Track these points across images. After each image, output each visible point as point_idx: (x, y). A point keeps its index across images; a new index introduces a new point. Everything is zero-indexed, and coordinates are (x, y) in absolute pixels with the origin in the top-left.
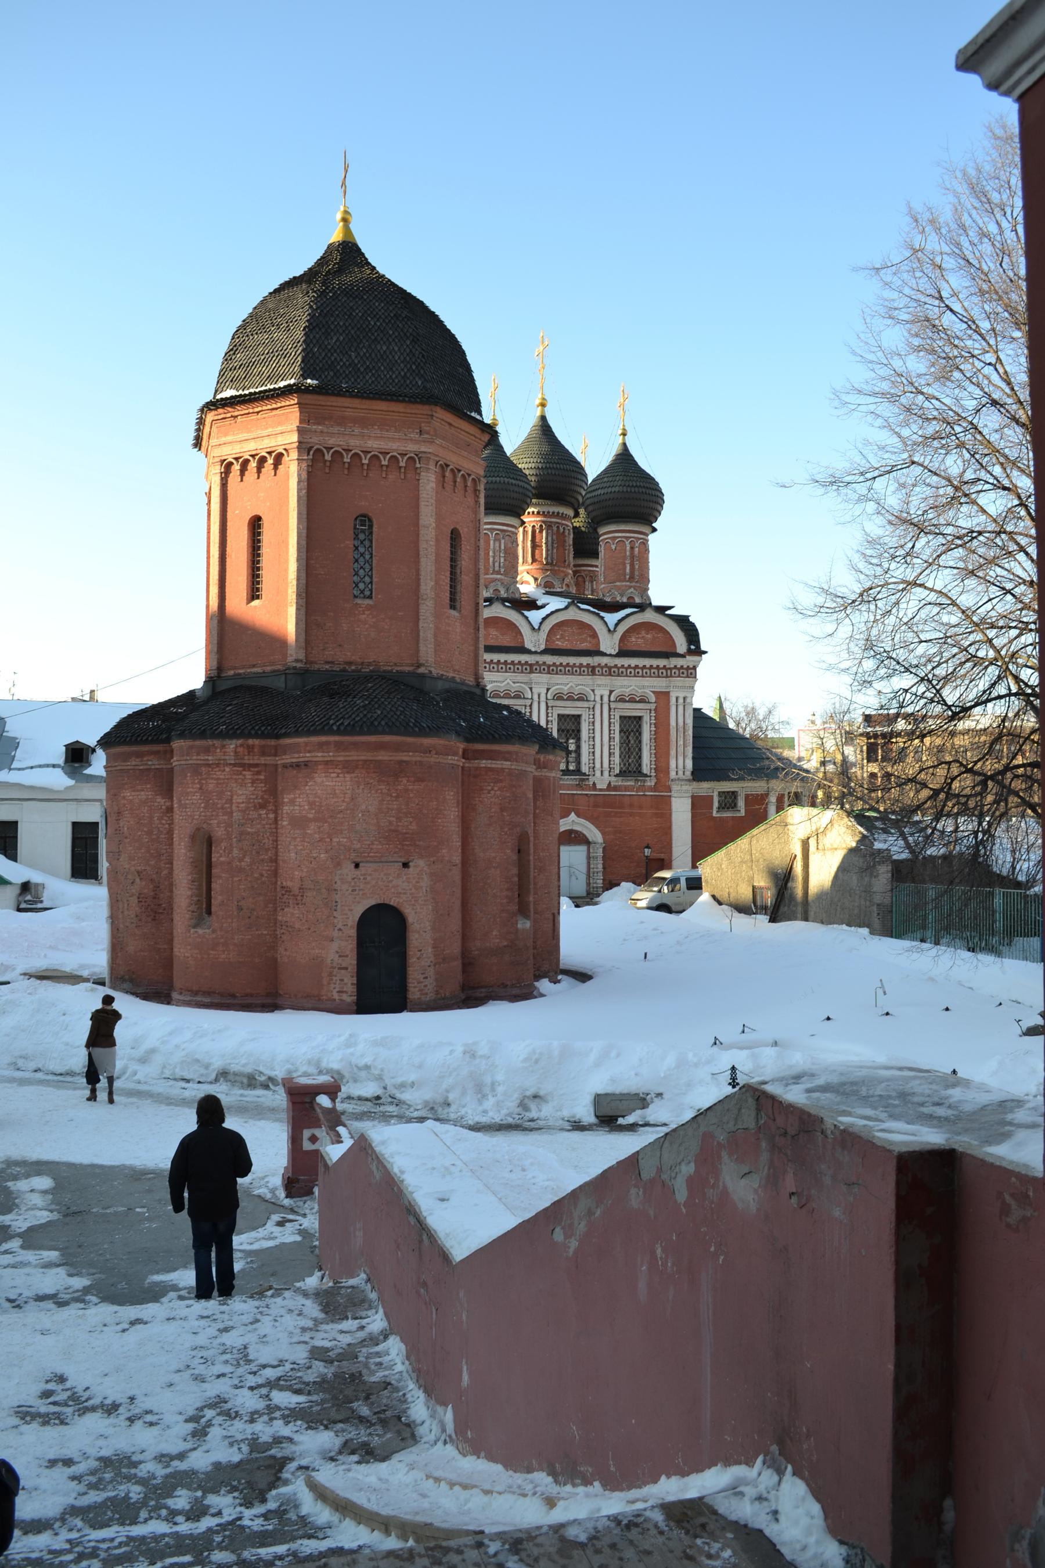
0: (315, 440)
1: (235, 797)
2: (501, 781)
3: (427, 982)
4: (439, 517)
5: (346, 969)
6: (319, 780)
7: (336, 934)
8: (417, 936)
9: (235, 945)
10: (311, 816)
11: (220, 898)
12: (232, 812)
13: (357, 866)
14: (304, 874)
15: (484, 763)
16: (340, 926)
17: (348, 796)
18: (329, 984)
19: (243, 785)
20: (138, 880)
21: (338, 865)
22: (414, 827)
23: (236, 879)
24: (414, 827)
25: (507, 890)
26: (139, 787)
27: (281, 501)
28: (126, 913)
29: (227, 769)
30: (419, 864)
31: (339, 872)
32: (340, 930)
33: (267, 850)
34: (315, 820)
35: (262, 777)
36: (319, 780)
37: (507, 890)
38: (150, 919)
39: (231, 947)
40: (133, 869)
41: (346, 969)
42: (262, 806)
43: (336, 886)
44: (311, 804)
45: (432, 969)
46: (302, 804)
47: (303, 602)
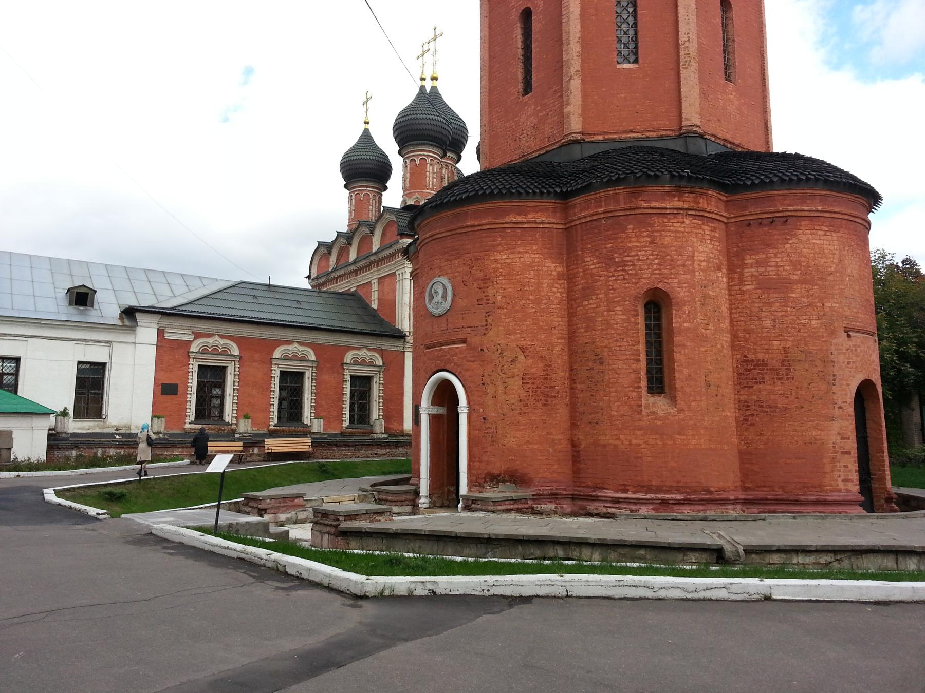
1: (696, 254)
5: (849, 453)
6: (804, 238)
7: (837, 412)
9: (705, 428)
10: (795, 277)
11: (686, 371)
12: (694, 271)
13: (849, 336)
14: (790, 344)
16: (839, 403)
17: (836, 256)
18: (833, 471)
19: (702, 241)
20: (521, 357)
21: (833, 333)
23: (702, 349)
26: (521, 249)
28: (502, 397)
29: (687, 221)
31: (834, 341)
32: (840, 407)
33: (725, 318)
34: (801, 282)
35: (717, 235)
36: (804, 238)
38: (539, 405)
39: (702, 431)
40: (513, 344)
41: (849, 453)
43: (832, 357)
46: (780, 264)
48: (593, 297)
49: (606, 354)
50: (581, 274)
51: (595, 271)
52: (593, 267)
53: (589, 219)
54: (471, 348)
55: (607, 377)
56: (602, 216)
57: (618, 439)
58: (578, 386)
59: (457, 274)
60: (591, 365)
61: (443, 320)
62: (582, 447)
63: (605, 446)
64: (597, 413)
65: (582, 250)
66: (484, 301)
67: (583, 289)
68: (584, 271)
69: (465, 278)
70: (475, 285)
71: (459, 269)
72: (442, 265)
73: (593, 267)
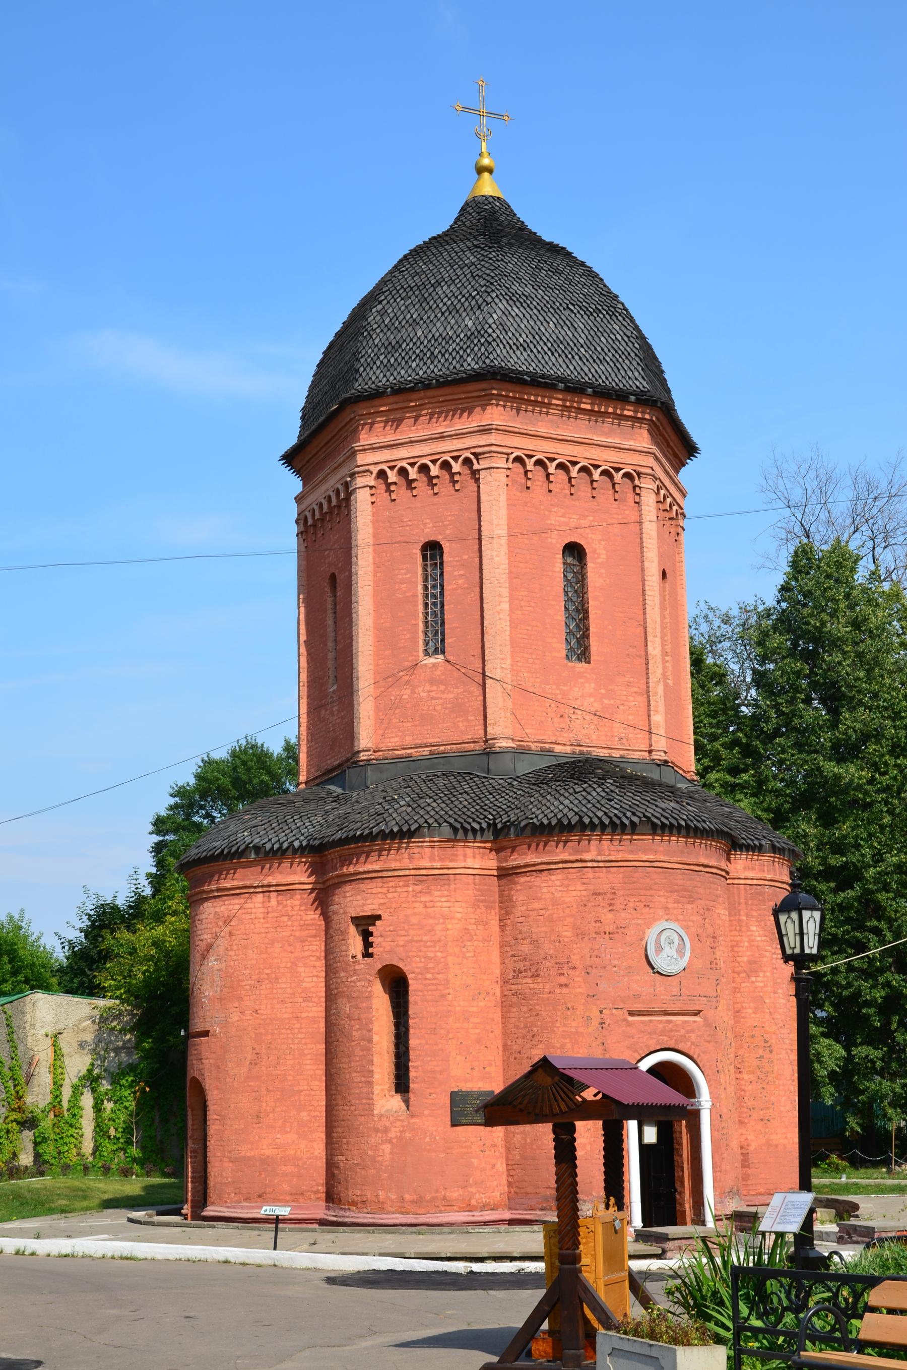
48: (761, 974)
49: (773, 1041)
50: (746, 944)
51: (761, 944)
52: (759, 939)
53: (755, 882)
54: (707, 1024)
55: (776, 1068)
56: (767, 883)
57: (786, 1138)
58: (746, 1077)
59: (691, 924)
60: (761, 1052)
61: (675, 981)
62: (752, 1148)
63: (776, 1146)
64: (768, 1108)
65: (747, 915)
66: (714, 966)
67: (750, 962)
68: (750, 941)
69: (700, 931)
70: (708, 943)
71: (691, 918)
72: (670, 906)
73: (759, 939)
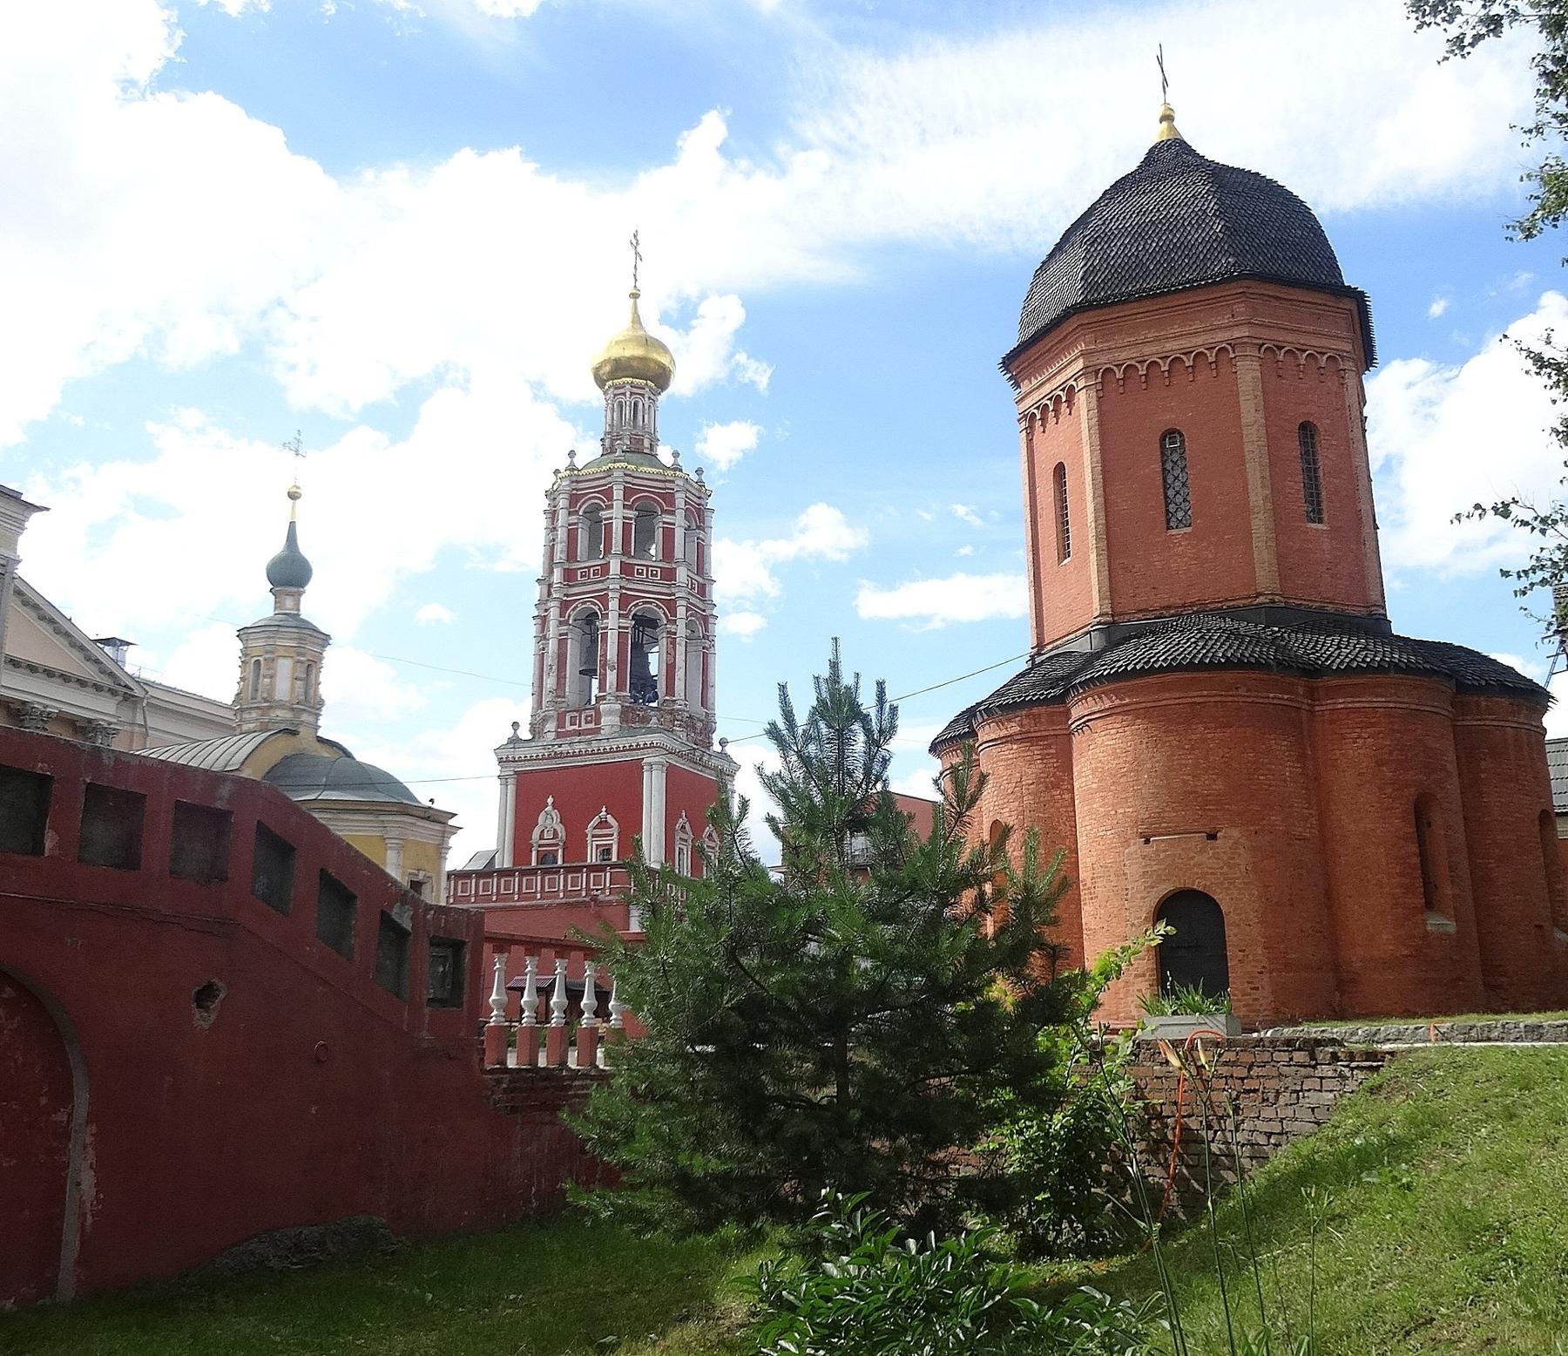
0: (1103, 360)
2: (1373, 725)
3: (1257, 994)
4: (1270, 409)
8: (1236, 930)
13: (1147, 842)
15: (1341, 703)
22: (1219, 786)
24: (1219, 786)
25: (1401, 875)
27: (1076, 437)
30: (1230, 835)
37: (1401, 875)
42: (1056, 786)
44: (1094, 771)
45: (1266, 977)
47: (1103, 544)
